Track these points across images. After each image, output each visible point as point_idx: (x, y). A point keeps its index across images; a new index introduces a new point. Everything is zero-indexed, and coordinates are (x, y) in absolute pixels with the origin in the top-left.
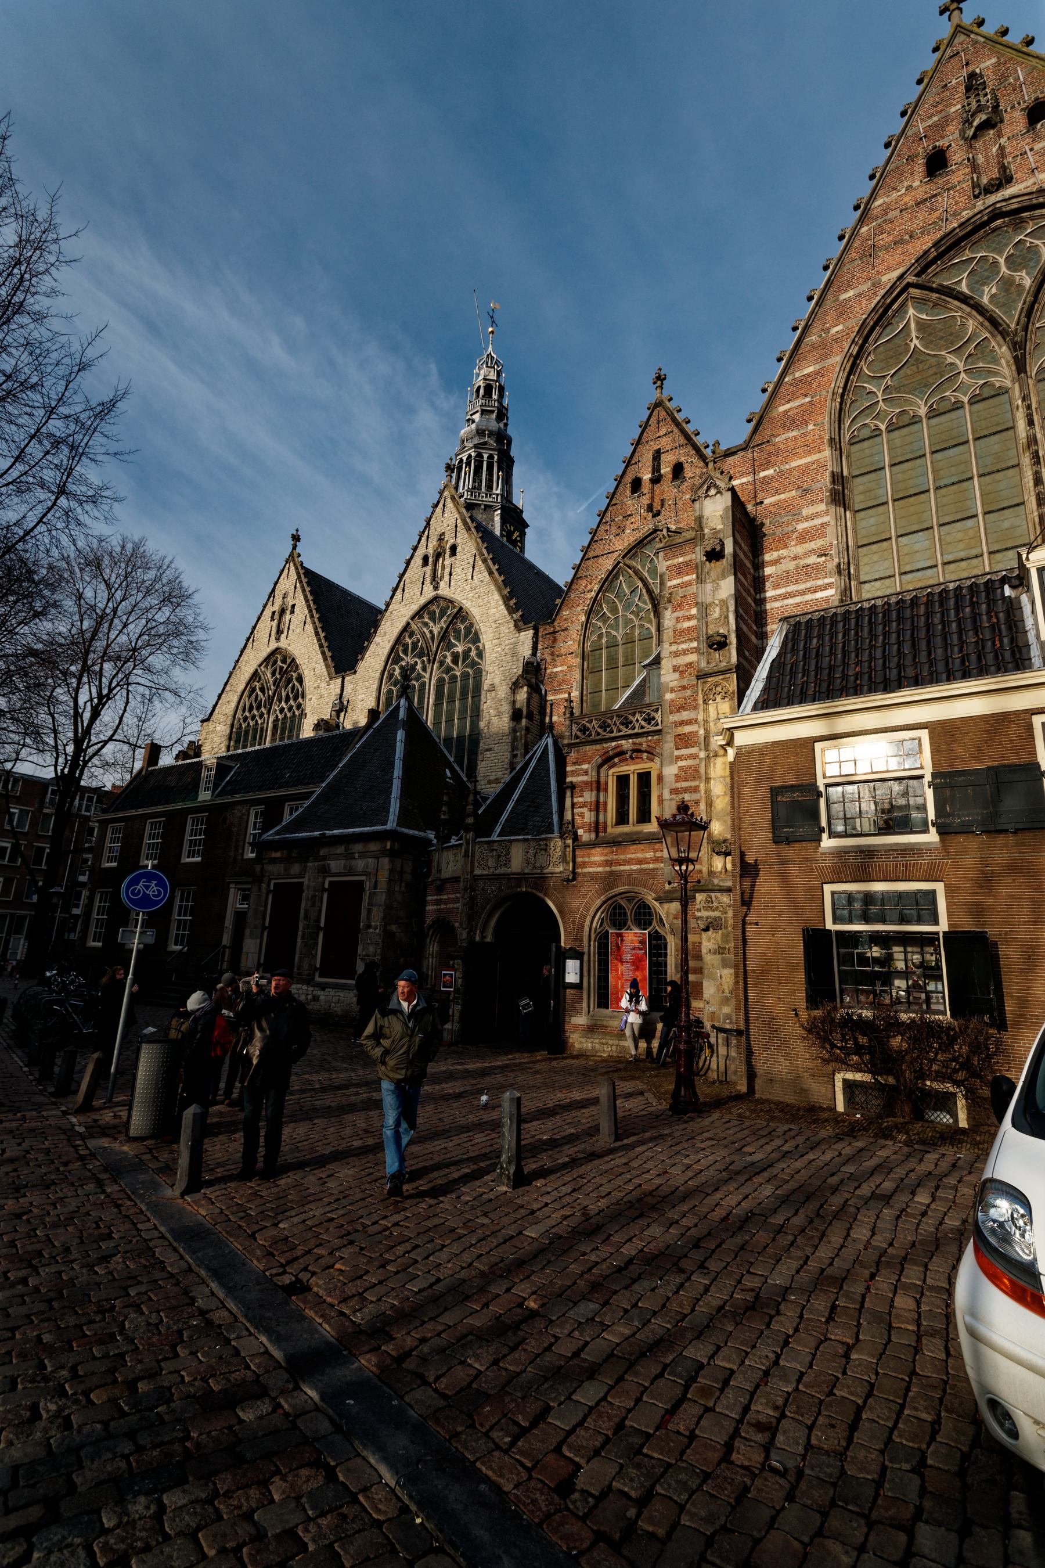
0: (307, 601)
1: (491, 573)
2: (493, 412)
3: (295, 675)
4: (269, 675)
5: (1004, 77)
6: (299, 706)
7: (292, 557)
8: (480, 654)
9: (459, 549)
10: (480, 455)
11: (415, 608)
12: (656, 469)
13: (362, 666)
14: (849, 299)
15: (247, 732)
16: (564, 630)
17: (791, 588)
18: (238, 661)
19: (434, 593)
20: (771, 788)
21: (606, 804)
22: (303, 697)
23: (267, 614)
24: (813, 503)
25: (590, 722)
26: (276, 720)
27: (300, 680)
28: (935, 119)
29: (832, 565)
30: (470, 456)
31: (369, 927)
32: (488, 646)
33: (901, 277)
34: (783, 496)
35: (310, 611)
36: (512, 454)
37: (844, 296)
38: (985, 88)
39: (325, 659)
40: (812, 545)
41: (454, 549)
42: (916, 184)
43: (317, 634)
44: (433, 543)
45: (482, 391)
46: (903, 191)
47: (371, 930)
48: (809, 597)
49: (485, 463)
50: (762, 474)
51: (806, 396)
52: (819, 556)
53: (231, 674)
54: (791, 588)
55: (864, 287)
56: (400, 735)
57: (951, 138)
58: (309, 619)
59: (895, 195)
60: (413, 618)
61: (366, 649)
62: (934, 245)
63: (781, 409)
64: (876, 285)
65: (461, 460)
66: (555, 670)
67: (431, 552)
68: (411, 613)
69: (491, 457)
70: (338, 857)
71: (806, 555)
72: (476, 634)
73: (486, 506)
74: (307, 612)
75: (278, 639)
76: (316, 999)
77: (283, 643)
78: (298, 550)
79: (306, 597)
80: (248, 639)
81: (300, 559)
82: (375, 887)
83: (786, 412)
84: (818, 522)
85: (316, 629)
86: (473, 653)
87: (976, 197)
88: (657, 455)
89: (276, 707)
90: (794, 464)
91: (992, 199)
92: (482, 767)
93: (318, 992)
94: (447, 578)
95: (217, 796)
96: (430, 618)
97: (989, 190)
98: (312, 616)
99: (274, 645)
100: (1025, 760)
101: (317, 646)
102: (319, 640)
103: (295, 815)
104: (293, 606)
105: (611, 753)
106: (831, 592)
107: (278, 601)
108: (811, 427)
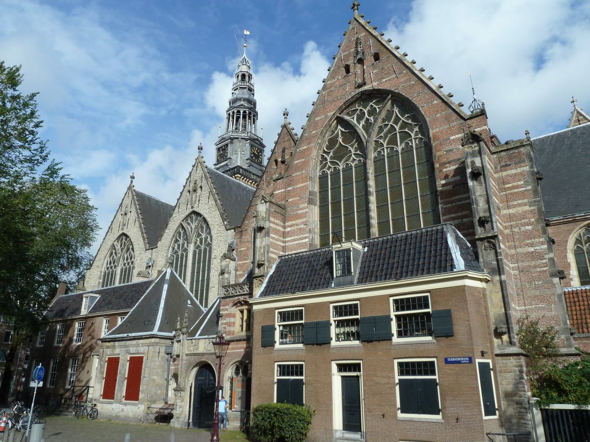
0: (137, 210)
1: (216, 201)
2: (246, 88)
3: (131, 247)
4: (119, 246)
5: (366, 41)
6: (132, 263)
7: (130, 188)
8: (211, 240)
10: (239, 112)
11: (184, 216)
12: (283, 157)
14: (318, 121)
15: (108, 275)
16: (245, 230)
17: (296, 237)
18: (104, 239)
19: (192, 210)
20: (263, 327)
21: (234, 323)
22: (134, 258)
23: (119, 215)
24: (303, 203)
25: (229, 288)
26: (122, 270)
27: (133, 249)
28: (347, 53)
29: (308, 229)
30: (233, 112)
31: (144, 377)
32: (214, 238)
33: (334, 114)
34: (294, 199)
35: (138, 215)
36: (256, 110)
37: (316, 119)
38: (360, 45)
39: (144, 240)
40: (302, 220)
41: (201, 187)
42: (340, 78)
43: (140, 227)
44: (192, 185)
45: (240, 78)
46: (336, 79)
47: (145, 379)
48: (300, 241)
49: (241, 115)
50: (288, 189)
51: (303, 158)
52: (304, 225)
53: (101, 245)
54: (296, 237)
55: (323, 117)
56: (166, 287)
57: (350, 62)
58: (137, 219)
59: (334, 81)
60: (183, 221)
61: (162, 235)
62: (344, 104)
63: (296, 162)
64: (326, 116)
65: (229, 114)
66: (242, 249)
67: (191, 190)
68: (182, 218)
69: (245, 112)
70: (133, 346)
71: (300, 224)
73: (242, 138)
74: (136, 215)
75: (122, 229)
76: (122, 410)
77: (125, 231)
78: (133, 184)
79: (136, 208)
80: (109, 228)
81: (134, 188)
82: (147, 360)
83: (297, 163)
84: (305, 211)
85: (140, 224)
86: (209, 239)
87: (356, 88)
88: (283, 151)
89: (121, 262)
90: (298, 186)
91: (361, 89)
93: (124, 407)
95: (89, 312)
96: (191, 221)
97: (360, 86)
98: (139, 218)
99: (121, 232)
100: (325, 320)
101: (140, 233)
102: (141, 230)
103: (123, 320)
105: (236, 302)
106: (307, 240)
107: (124, 209)
108: (304, 171)
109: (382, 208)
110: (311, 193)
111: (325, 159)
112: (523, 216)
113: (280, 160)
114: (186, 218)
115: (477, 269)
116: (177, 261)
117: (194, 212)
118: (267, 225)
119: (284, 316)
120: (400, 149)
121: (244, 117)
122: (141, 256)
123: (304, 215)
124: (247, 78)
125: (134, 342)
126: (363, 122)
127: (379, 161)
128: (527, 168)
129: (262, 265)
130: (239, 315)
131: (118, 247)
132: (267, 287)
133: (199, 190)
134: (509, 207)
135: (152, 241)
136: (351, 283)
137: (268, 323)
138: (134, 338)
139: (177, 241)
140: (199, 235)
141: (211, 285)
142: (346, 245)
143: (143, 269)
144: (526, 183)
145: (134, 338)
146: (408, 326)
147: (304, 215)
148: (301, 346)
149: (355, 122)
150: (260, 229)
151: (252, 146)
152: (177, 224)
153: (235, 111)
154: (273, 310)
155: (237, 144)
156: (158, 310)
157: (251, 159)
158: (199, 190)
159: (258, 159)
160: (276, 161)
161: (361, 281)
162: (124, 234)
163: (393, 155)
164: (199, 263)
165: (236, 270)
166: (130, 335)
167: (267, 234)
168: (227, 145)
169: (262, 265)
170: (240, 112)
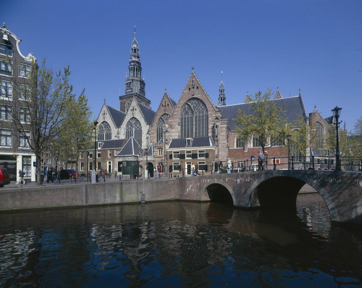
6: (110, 132)
8: (141, 127)
9: (137, 110)
10: (134, 67)
11: (130, 118)
12: (165, 104)
13: (122, 127)
23: (101, 114)
26: (106, 134)
27: (110, 127)
30: (132, 67)
32: (142, 127)
41: (136, 109)
65: (130, 68)
68: (129, 119)
69: (137, 68)
72: (140, 124)
77: (105, 120)
88: (165, 102)
89: (105, 131)
92: (143, 145)
94: (135, 114)
97: (193, 95)
98: (111, 116)
99: (103, 120)
102: (113, 121)
104: (107, 114)
109: (196, 129)
110: (179, 122)
111: (182, 114)
112: (224, 135)
113: (164, 105)
114: (131, 119)
115: (214, 146)
116: (128, 134)
117: (133, 117)
118: (168, 130)
119: (174, 153)
120: (201, 115)
121: (137, 70)
122: (114, 130)
123: (177, 128)
124: (137, 52)
125: (127, 157)
126: (193, 106)
127: (196, 117)
128: (226, 126)
129: (167, 140)
130: (158, 151)
131: (103, 126)
132: (170, 146)
133: (135, 110)
134: (222, 133)
135: (118, 124)
136: (190, 147)
137: (171, 154)
138: (127, 156)
139: (127, 126)
140: (136, 125)
141: (142, 141)
142: (189, 139)
143: (116, 134)
144: (226, 129)
145: (127, 156)
146: (201, 156)
147: (177, 128)
148: (179, 159)
149: (191, 105)
150: (167, 131)
151: (140, 84)
152: (128, 120)
153: (133, 67)
154: (172, 151)
155: (134, 82)
156: (132, 149)
157: (140, 90)
158: (135, 110)
159: (143, 89)
160: (163, 105)
161: (192, 147)
162: (104, 121)
163: (199, 116)
164: (137, 134)
165: (151, 138)
166: (125, 155)
167: (168, 133)
168: (130, 82)
169: (167, 140)
170: (135, 68)
